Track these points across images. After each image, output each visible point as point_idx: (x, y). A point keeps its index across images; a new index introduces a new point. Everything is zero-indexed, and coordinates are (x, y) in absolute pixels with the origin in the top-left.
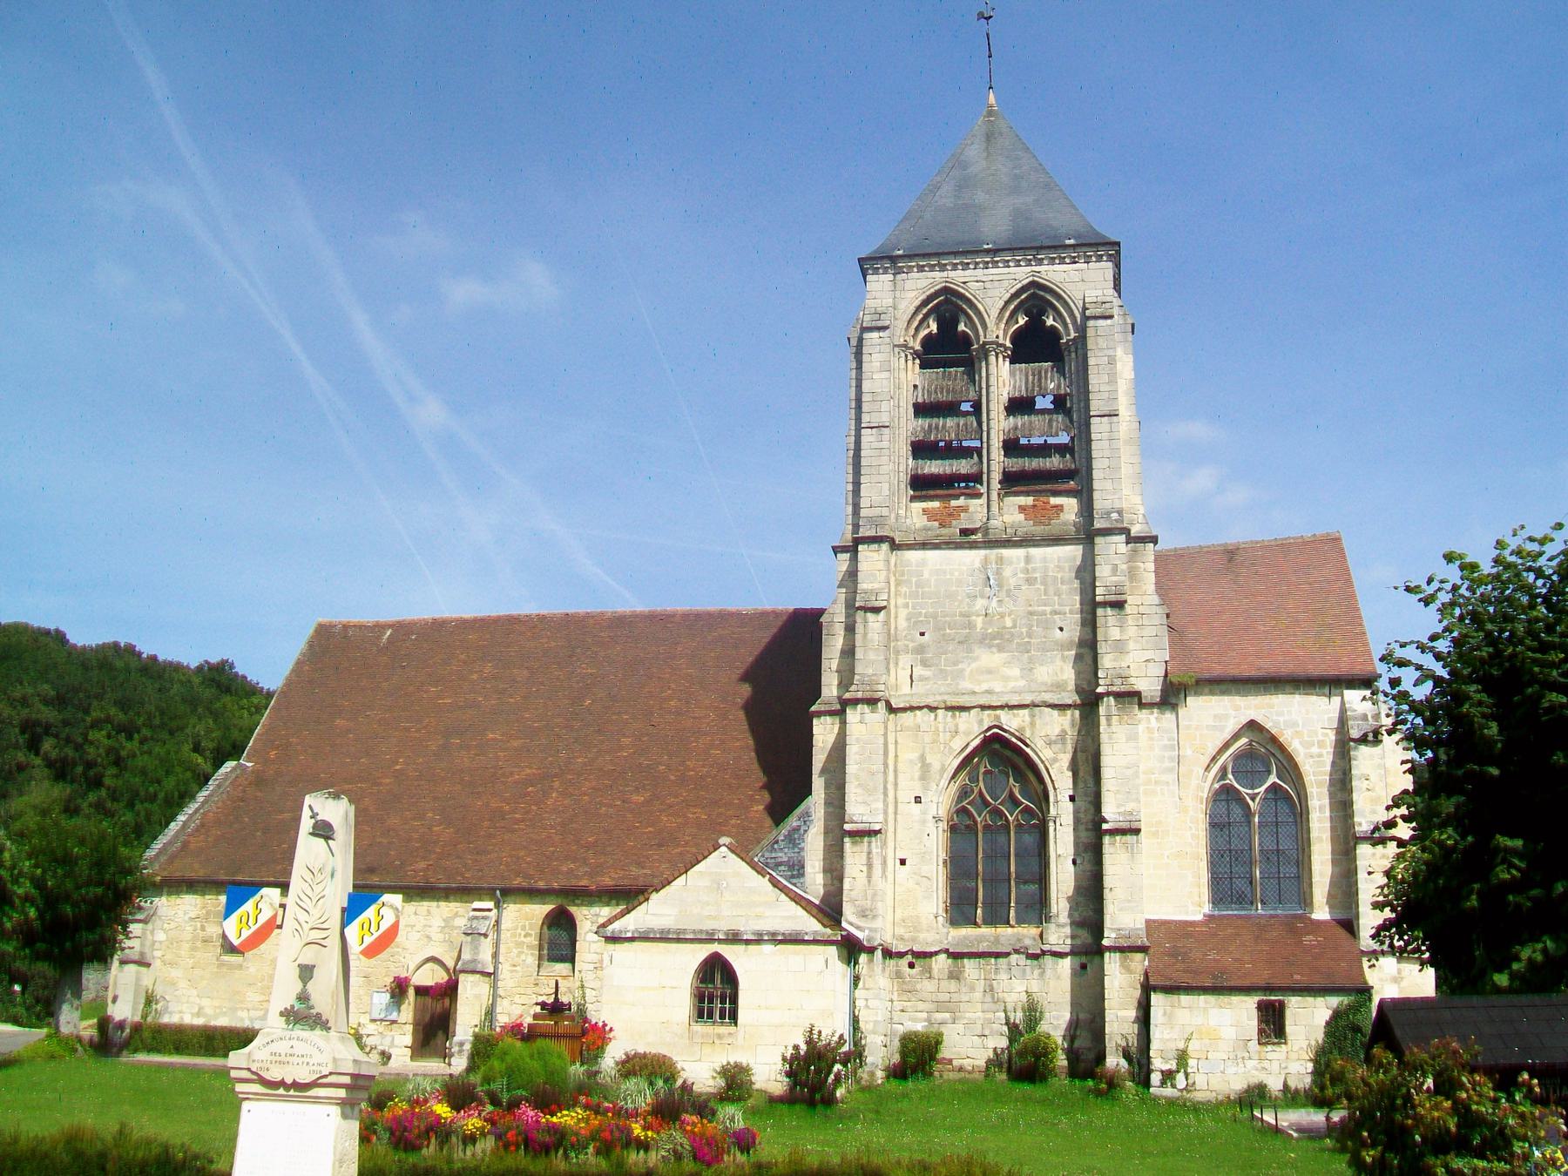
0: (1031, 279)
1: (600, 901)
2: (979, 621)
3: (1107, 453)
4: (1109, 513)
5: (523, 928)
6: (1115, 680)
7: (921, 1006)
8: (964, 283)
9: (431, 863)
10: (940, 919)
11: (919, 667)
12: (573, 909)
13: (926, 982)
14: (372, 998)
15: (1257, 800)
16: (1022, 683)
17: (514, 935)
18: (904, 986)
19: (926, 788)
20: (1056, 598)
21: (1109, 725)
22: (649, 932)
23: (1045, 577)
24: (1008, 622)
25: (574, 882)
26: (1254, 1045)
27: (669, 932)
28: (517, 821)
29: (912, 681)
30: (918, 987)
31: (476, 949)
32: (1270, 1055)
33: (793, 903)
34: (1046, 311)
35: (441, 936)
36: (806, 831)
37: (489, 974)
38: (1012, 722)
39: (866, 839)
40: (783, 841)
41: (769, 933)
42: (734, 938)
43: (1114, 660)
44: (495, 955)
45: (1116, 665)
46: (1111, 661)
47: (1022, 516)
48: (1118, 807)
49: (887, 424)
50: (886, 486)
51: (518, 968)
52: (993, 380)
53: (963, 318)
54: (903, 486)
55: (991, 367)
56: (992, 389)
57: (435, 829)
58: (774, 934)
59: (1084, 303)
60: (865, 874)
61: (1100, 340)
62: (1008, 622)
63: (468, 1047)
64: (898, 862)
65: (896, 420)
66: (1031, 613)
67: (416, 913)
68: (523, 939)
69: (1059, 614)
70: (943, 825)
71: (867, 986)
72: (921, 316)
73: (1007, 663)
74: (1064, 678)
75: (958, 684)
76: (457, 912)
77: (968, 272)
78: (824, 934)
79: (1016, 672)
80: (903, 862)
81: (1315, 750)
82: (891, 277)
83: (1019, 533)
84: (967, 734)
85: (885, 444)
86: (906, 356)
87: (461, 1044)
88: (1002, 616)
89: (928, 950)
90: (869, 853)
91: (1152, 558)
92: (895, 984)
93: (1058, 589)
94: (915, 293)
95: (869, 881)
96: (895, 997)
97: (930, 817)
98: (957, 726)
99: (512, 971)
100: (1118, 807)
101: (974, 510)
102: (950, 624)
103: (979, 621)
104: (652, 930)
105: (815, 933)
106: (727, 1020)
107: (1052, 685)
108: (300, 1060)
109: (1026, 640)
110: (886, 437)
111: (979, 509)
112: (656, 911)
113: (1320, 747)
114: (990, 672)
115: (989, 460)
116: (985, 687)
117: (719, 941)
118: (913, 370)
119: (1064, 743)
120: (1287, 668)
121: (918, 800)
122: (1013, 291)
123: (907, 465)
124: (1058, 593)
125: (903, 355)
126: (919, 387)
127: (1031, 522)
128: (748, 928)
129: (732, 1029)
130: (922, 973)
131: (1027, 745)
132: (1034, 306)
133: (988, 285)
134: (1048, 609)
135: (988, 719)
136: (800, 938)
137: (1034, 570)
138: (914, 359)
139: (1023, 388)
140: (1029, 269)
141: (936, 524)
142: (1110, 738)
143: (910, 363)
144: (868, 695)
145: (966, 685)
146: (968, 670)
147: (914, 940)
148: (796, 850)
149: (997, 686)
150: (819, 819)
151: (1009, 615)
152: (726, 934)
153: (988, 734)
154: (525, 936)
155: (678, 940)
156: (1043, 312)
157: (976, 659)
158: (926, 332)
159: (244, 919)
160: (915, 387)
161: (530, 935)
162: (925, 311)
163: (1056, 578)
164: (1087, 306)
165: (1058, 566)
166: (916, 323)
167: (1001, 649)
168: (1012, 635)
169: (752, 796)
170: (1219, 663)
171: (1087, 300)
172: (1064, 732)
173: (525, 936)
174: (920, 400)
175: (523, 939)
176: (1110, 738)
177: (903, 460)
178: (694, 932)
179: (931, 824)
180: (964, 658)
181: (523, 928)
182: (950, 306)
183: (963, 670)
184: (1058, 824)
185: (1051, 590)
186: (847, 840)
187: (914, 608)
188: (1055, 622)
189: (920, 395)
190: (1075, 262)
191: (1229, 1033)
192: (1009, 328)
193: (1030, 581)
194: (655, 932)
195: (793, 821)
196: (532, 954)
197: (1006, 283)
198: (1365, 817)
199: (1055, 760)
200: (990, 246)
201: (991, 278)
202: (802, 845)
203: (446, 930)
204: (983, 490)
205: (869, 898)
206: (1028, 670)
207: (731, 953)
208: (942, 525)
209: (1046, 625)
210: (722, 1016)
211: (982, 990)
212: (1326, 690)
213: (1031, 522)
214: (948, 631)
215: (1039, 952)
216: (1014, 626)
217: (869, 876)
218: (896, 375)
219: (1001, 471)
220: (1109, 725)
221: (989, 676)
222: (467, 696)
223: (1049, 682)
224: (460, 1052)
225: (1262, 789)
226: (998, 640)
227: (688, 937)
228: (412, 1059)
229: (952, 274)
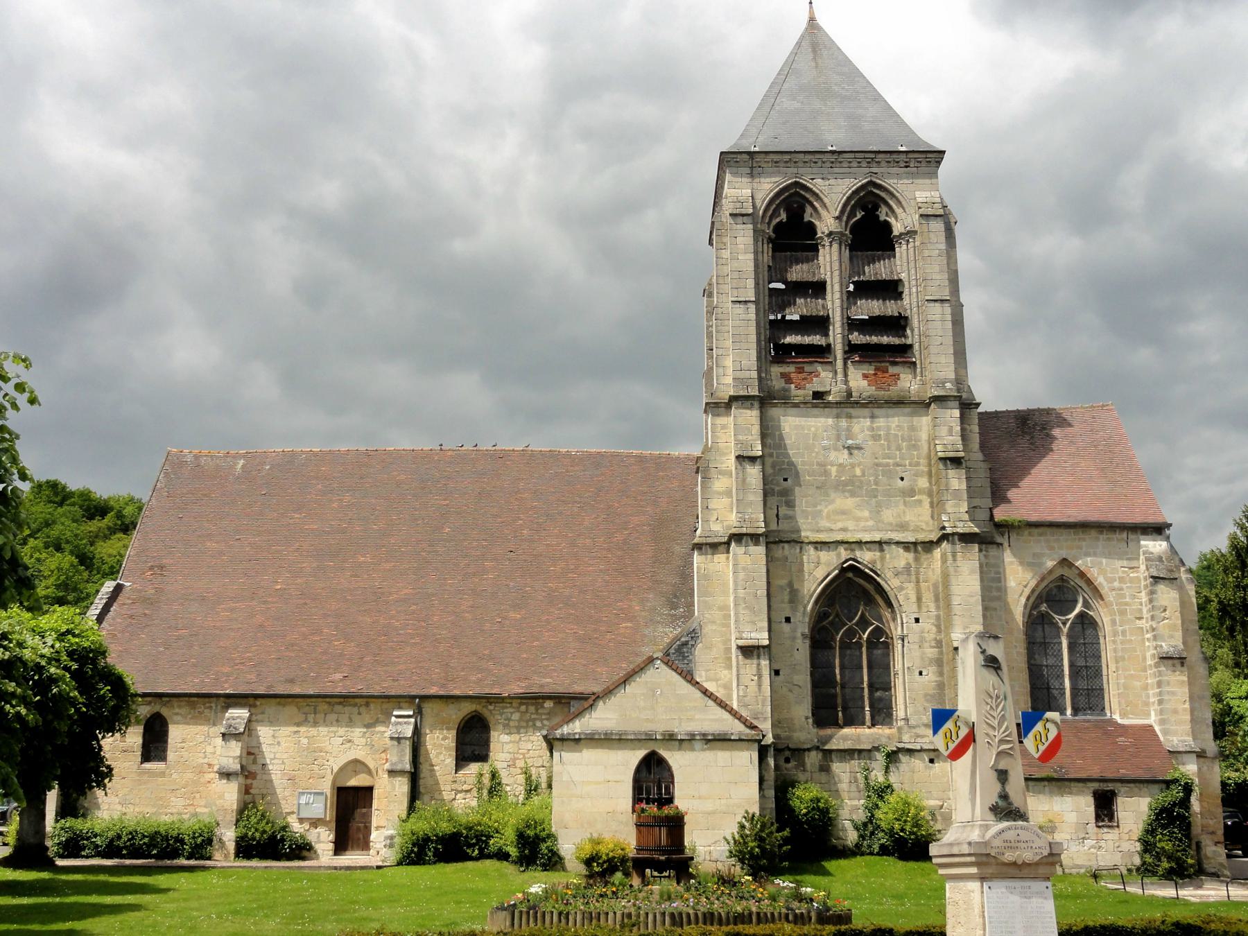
0: (869, 179)
2: (834, 470)
4: (944, 383)
6: (958, 523)
8: (812, 179)
10: (810, 721)
11: (784, 508)
15: (1068, 626)
16: (871, 523)
19: (794, 610)
20: (898, 453)
21: (955, 560)
22: (594, 734)
23: (888, 435)
24: (858, 472)
26: (1092, 827)
27: (612, 734)
29: (778, 519)
32: (1106, 837)
34: (880, 206)
36: (693, 645)
38: (866, 557)
40: (674, 654)
42: (670, 738)
43: (954, 506)
45: (956, 510)
46: (952, 507)
48: (964, 629)
53: (809, 210)
58: (704, 735)
61: (932, 235)
62: (858, 472)
64: (773, 673)
66: (877, 465)
69: (901, 466)
70: (808, 642)
72: (774, 206)
73: (858, 506)
74: (907, 519)
75: (817, 523)
78: (748, 734)
79: (866, 514)
81: (1116, 584)
84: (828, 564)
86: (763, 240)
88: (853, 466)
91: (977, 421)
93: (899, 445)
95: (760, 689)
97: (799, 635)
98: (819, 557)
100: (964, 629)
101: (825, 378)
102: (808, 472)
103: (834, 470)
105: (740, 733)
107: (897, 525)
108: (1025, 845)
109: (874, 487)
112: (601, 718)
113: (1120, 582)
114: (843, 512)
116: (840, 525)
119: (909, 574)
120: (1093, 516)
121: (788, 620)
124: (899, 448)
127: (874, 388)
128: (681, 729)
131: (878, 575)
134: (891, 461)
135: (844, 554)
136: (728, 737)
137: (879, 428)
140: (867, 170)
142: (956, 571)
143: (765, 246)
144: (750, 531)
145: (824, 523)
146: (826, 511)
148: (686, 662)
149: (850, 525)
151: (859, 466)
152: (663, 735)
153: (845, 566)
154: (442, 739)
156: (876, 207)
157: (833, 501)
158: (778, 220)
159: (1038, 737)
162: (778, 202)
163: (896, 435)
165: (897, 426)
167: (853, 494)
168: (861, 482)
170: (1035, 511)
172: (908, 564)
176: (956, 571)
179: (799, 641)
180: (821, 500)
182: (798, 199)
183: (820, 511)
184: (906, 641)
185: (893, 448)
187: (777, 457)
188: (897, 472)
191: (1071, 818)
193: (876, 438)
194: (600, 734)
198: (1164, 641)
199: (901, 589)
202: (691, 657)
206: (877, 511)
209: (889, 474)
211: (848, 781)
212: (1125, 535)
213: (874, 388)
214: (807, 478)
215: (895, 749)
216: (863, 475)
220: (955, 560)
221: (844, 517)
222: (333, 523)
223: (894, 523)
225: (1072, 616)
226: (849, 486)
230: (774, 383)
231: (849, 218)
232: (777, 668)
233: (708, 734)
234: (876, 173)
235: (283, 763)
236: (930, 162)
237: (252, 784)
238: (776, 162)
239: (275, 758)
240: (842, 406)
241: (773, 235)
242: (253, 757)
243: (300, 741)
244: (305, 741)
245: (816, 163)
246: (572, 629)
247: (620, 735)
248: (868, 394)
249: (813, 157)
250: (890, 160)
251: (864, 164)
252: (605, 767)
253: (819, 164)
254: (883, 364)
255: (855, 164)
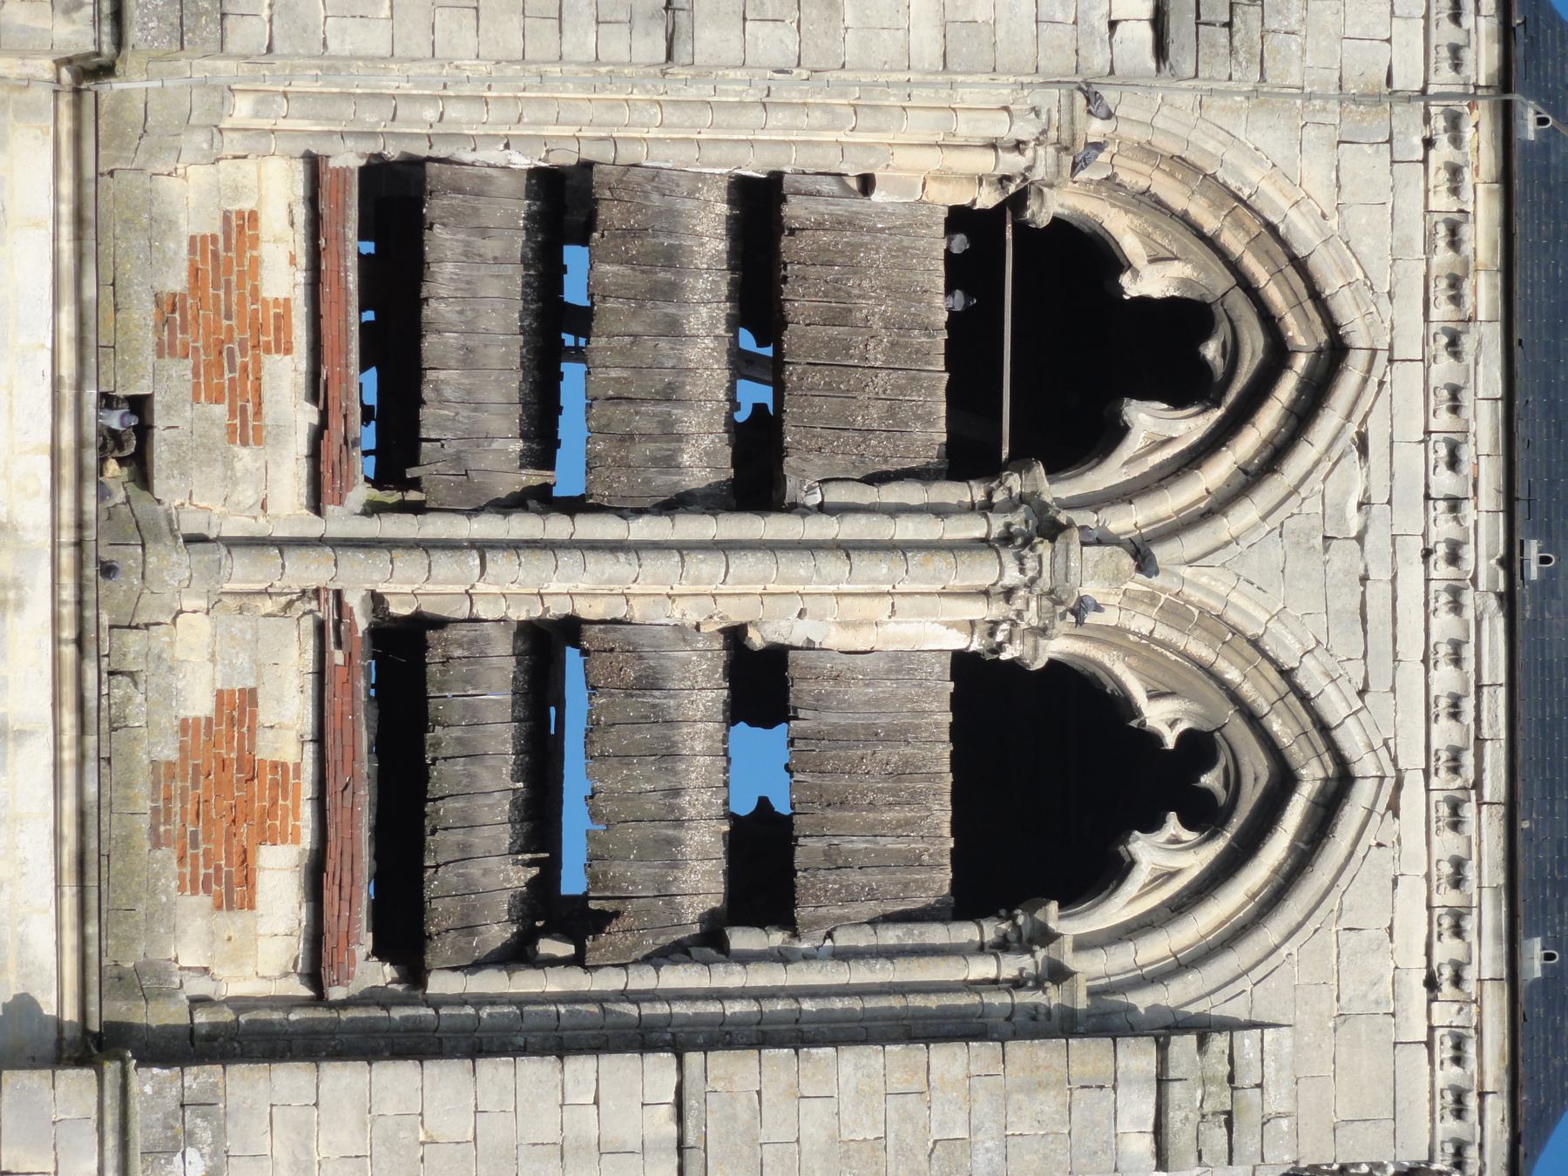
3: (496, 1131)
47: (200, 704)
49: (681, 52)
50: (374, 40)
52: (879, 570)
53: (1191, 426)
54: (371, 118)
55: (940, 562)
56: (833, 566)
59: (1230, 1026)
61: (1049, 1103)
65: (704, 91)
77: (1411, 459)
82: (1409, 77)
83: (121, 688)
85: (582, 39)
86: (1018, 146)
94: (1323, 196)
110: (616, 46)
111: (247, 495)
115: (482, 547)
118: (942, 177)
122: (1311, 677)
123: (474, 141)
125: (1026, 129)
126: (858, 205)
132: (1234, 783)
133: (1343, 557)
138: (1004, 180)
139: (832, 718)
140: (1413, 759)
141: (176, 281)
143: (985, 162)
158: (1131, 246)
160: (867, 184)
164: (1219, 1042)
166: (1175, 195)
171: (1247, 1042)
174: (794, 210)
177: (496, 120)
189: (821, 206)
190: (1431, 983)
192: (1128, 651)
197: (1347, 642)
200: (1534, 571)
201: (1380, 574)
204: (343, 520)
208: (168, 307)
218: (921, 96)
219: (431, 607)
229: (1407, 380)
230: (199, 175)
231: (1145, 650)
234: (1394, 808)
236: (1459, 1113)
238: (1454, 231)
240: (67, 557)
241: (1040, 214)
245: (1453, 462)
248: (137, 715)
249: (1485, 447)
250: (1471, 885)
251: (1446, 733)
253: (1445, 482)
254: (307, 812)
255: (1445, 679)
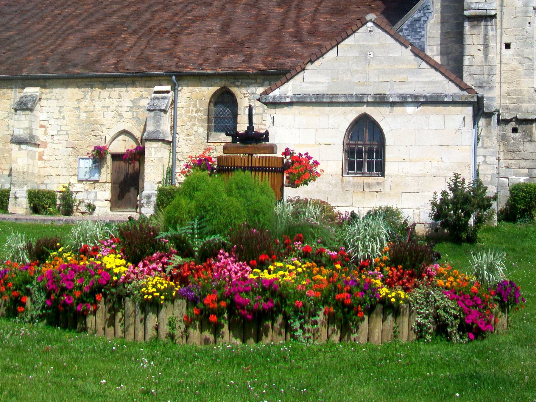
1: (256, 83)
5: (195, 105)
7: (523, 163)
9: (120, 59)
12: (234, 90)
13: (527, 144)
14: (79, 165)
17: (187, 111)
18: (509, 148)
22: (305, 97)
25: (234, 68)
27: (323, 96)
28: (187, 28)
30: (521, 148)
31: (158, 122)
33: (433, 70)
35: (130, 114)
36: (425, 21)
37: (169, 143)
39: (483, 23)
40: (406, 29)
41: (412, 96)
44: (173, 128)
51: (192, 137)
57: (123, 36)
58: (417, 97)
60: (482, 53)
63: (154, 199)
64: (504, 46)
67: (110, 97)
68: (194, 114)
71: (485, 145)
76: (142, 95)
78: (461, 96)
80: (508, 46)
87: (149, 197)
89: (530, 117)
90: (486, 35)
92: (501, 145)
96: (501, 156)
99: (187, 140)
104: (307, 96)
105: (453, 95)
106: (374, 172)
117: (368, 104)
129: (380, 179)
130: (524, 136)
136: (440, 100)
147: (517, 109)
148: (418, 37)
150: (437, 12)
152: (375, 96)
154: (196, 112)
155: (331, 104)
161: (201, 111)
169: (369, 5)
173: (196, 112)
175: (194, 114)
178: (345, 96)
181: (195, 105)
186: (466, 24)
195: (415, 13)
196: (202, 126)
202: (423, 33)
203: (134, 110)
205: (486, 71)
207: (375, 113)
210: (370, 169)
217: (486, 55)
224: (148, 203)
227: (340, 100)
228: (112, 209)
232: (508, 41)
233: (421, 97)
235: (68, 134)
237: (43, 152)
239: (61, 130)
242: (44, 129)
243: (80, 115)
244: (84, 115)
246: (326, 18)
247: (331, 98)
252: (316, 130)
